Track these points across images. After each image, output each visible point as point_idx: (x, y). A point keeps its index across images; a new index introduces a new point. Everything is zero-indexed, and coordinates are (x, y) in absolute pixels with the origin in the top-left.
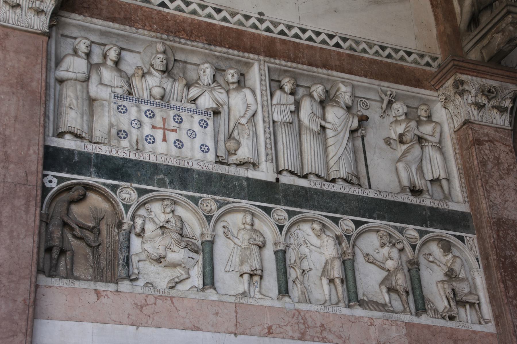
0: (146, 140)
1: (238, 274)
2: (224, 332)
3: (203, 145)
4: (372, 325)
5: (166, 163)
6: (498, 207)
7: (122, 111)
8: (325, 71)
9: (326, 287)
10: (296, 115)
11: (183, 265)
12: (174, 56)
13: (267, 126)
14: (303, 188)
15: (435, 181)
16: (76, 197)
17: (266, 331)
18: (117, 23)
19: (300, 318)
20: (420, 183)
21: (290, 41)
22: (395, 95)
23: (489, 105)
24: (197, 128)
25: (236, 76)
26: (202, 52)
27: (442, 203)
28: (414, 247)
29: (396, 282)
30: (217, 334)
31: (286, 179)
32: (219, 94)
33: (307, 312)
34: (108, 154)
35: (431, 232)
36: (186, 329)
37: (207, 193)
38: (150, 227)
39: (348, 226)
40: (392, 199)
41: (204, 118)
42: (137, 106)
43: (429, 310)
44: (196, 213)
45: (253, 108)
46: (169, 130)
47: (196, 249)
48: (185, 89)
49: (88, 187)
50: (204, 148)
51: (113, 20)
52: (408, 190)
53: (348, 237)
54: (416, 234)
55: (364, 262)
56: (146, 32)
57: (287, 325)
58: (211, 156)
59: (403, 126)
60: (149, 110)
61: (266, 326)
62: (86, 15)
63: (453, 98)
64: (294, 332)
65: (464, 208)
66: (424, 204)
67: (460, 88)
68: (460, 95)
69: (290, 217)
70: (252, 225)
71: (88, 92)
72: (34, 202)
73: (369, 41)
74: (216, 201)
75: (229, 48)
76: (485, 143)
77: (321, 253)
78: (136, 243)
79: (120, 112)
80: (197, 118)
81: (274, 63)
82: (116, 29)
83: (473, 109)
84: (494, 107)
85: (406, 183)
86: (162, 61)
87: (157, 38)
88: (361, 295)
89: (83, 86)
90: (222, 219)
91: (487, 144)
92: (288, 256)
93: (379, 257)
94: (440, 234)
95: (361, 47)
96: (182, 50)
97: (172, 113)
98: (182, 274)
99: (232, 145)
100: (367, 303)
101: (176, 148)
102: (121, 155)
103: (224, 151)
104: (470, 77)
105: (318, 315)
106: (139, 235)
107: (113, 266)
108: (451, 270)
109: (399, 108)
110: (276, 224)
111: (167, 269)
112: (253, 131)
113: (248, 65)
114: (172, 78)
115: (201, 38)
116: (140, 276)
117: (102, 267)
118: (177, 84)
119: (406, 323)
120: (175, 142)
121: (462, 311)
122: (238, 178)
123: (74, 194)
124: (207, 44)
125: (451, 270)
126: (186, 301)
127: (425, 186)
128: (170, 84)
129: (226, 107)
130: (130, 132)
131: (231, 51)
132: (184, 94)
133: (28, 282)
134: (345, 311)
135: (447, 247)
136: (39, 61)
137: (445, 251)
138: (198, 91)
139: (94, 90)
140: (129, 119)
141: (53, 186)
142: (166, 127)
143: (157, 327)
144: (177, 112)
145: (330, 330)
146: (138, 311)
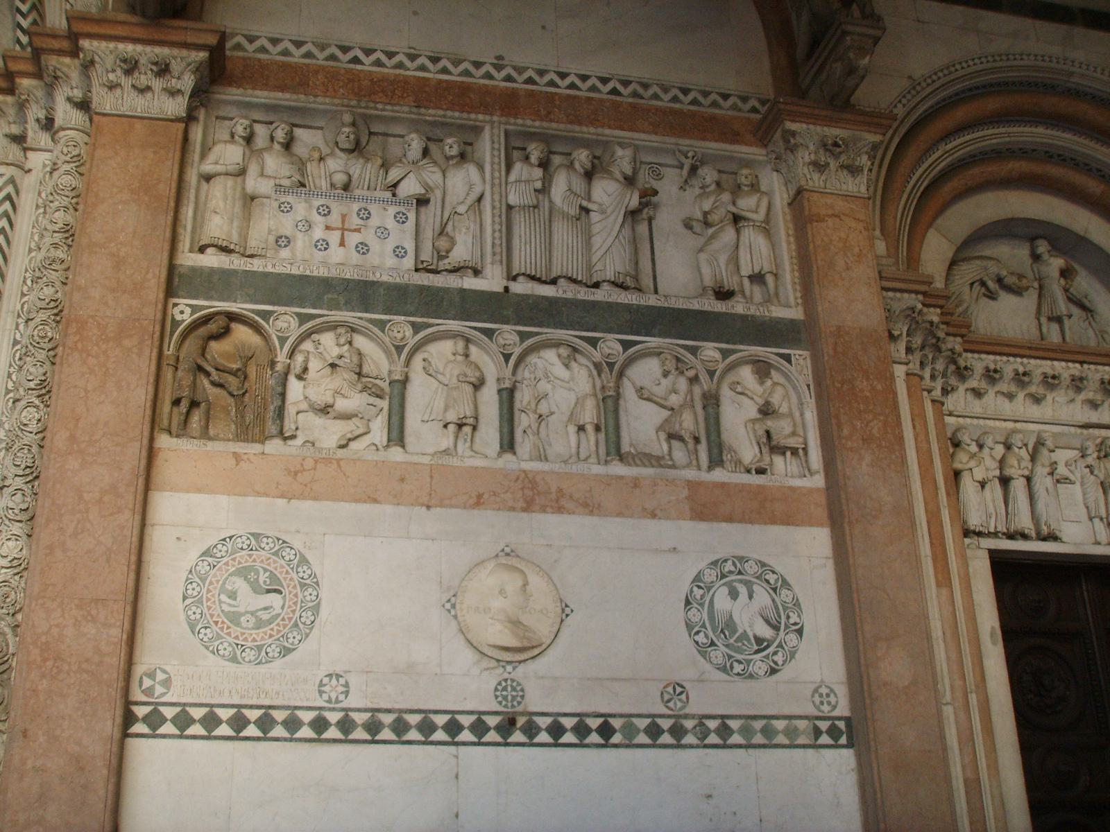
0: (316, 246)
1: (442, 424)
2: (412, 505)
3: (398, 247)
5: (342, 276)
7: (285, 210)
8: (592, 130)
9: (573, 438)
10: (547, 196)
11: (360, 416)
12: (368, 128)
13: (497, 212)
15: (757, 278)
16: (215, 331)
17: (475, 500)
18: (288, 92)
19: (526, 481)
20: (730, 282)
21: (541, 92)
22: (700, 156)
23: (833, 164)
24: (391, 224)
25: (455, 146)
26: (407, 118)
27: (761, 309)
28: (711, 373)
29: (681, 425)
30: (402, 508)
31: (520, 287)
32: (430, 174)
33: (538, 473)
34: (261, 269)
35: (741, 351)
36: (356, 501)
37: (400, 315)
38: (314, 365)
39: (613, 349)
40: (685, 307)
41: (402, 209)
42: (306, 201)
43: (728, 463)
45: (477, 190)
46: (350, 230)
47: (378, 392)
48: (381, 172)
49: (232, 317)
50: (399, 252)
51: (282, 88)
52: (711, 292)
53: (611, 365)
54: (718, 355)
55: (636, 399)
56: (327, 100)
57: (507, 492)
58: (409, 262)
59: (712, 199)
60: (322, 206)
62: (247, 87)
63: (784, 157)
65: (796, 313)
66: (734, 312)
67: (792, 141)
68: (792, 152)
69: (522, 341)
70: (467, 356)
71: (244, 189)
72: (150, 342)
73: (664, 83)
74: (413, 324)
75: (447, 109)
76: (826, 219)
77: (570, 389)
78: (295, 388)
79: (283, 211)
80: (392, 210)
81: (515, 124)
82: (287, 100)
83: (811, 170)
84: (842, 167)
85: (708, 281)
86: (348, 137)
87: (343, 106)
88: (628, 446)
89: (236, 183)
90: (423, 349)
91: (830, 222)
92: (518, 395)
93: (659, 391)
94: (753, 352)
95: (651, 92)
96: (377, 117)
97: (356, 207)
98: (358, 427)
99: (443, 243)
100: (633, 457)
101: (358, 255)
102: (279, 269)
103: (430, 254)
104: (804, 126)
106: (300, 377)
107: (260, 418)
108: (767, 403)
109: (708, 174)
110: (501, 353)
111: (338, 422)
112: (475, 222)
113: (477, 130)
114: (363, 157)
115: (406, 100)
116: (299, 433)
117: (248, 421)
118: (369, 165)
119: (689, 481)
120: (357, 247)
121: (778, 461)
122: (446, 290)
123: (213, 327)
124: (416, 107)
125: (767, 403)
127: (738, 285)
128: (359, 166)
129: (438, 193)
130: (294, 237)
131: (449, 113)
132: (380, 178)
133: (137, 445)
134: (598, 469)
135: (763, 370)
136: (171, 155)
137: (760, 377)
138: (400, 172)
139: (253, 183)
140: (294, 220)
141: (185, 318)
142: (345, 227)
143: (315, 499)
144: (363, 205)
145: (571, 497)
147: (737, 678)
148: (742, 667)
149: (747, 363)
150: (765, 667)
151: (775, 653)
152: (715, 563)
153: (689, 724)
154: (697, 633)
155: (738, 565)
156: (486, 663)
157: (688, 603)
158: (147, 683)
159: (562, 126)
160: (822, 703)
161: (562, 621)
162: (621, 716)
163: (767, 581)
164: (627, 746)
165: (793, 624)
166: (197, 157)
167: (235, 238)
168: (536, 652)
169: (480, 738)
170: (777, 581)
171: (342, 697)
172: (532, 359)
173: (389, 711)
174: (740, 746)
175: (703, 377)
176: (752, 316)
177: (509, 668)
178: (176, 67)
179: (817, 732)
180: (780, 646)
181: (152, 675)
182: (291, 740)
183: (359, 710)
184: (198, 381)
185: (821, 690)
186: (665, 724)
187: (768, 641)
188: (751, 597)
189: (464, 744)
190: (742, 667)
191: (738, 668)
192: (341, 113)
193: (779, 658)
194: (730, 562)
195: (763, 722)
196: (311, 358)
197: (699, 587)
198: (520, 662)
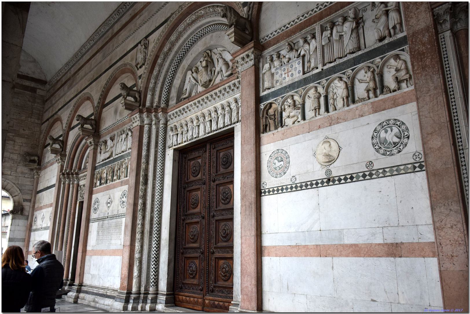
4: (357, 109)
6: (414, 26)
12: (293, 43)
14: (332, 67)
24: (297, 66)
28: (378, 67)
36: (295, 136)
38: (286, 107)
40: (369, 50)
44: (298, 96)
45: (315, 46)
49: (271, 104)
54: (380, 60)
58: (301, 73)
61: (318, 126)
64: (327, 124)
78: (284, 114)
80: (297, 62)
81: (322, 22)
96: (294, 39)
102: (277, 88)
105: (336, 114)
111: (292, 118)
113: (314, 29)
122: (310, 77)
123: (267, 108)
126: (295, 127)
130: (279, 79)
135: (397, 57)
144: (291, 64)
145: (340, 118)
146: (283, 135)
147: (388, 156)
148: (389, 152)
149: (392, 57)
150: (397, 151)
151: (400, 146)
152: (380, 124)
153: (374, 172)
154: (376, 146)
155: (388, 122)
156: (323, 167)
157: (372, 138)
158: (263, 185)
159: (334, 14)
160: (416, 158)
161: (339, 152)
162: (356, 173)
163: (397, 125)
164: (357, 181)
165: (406, 136)
166: (261, 70)
167: (270, 85)
168: (333, 161)
169: (323, 185)
170: (400, 123)
171: (295, 181)
172: (332, 84)
173: (304, 182)
174: (389, 176)
175: (376, 68)
176: (391, 42)
177: (328, 167)
178: (250, 54)
179: (415, 167)
180: (402, 143)
181: (264, 184)
182: (287, 192)
183: (298, 183)
184: (267, 119)
185: (416, 154)
186: (367, 173)
187: (397, 143)
188: (392, 131)
189: (319, 187)
190: (389, 152)
191: (388, 153)
192: (285, 43)
193: (401, 147)
194: (385, 122)
195: (396, 168)
196: (285, 106)
197: (376, 132)
198: (330, 165)
